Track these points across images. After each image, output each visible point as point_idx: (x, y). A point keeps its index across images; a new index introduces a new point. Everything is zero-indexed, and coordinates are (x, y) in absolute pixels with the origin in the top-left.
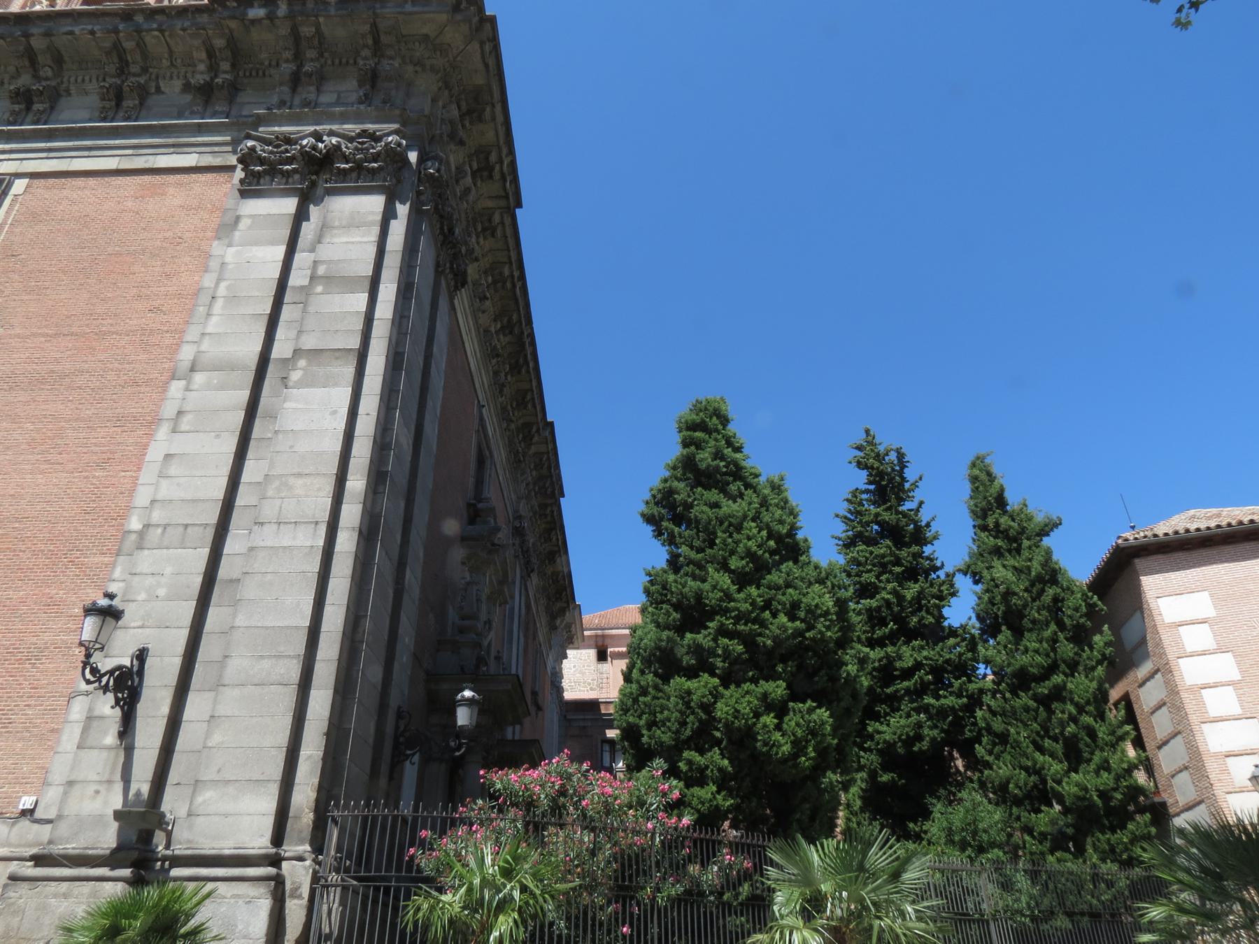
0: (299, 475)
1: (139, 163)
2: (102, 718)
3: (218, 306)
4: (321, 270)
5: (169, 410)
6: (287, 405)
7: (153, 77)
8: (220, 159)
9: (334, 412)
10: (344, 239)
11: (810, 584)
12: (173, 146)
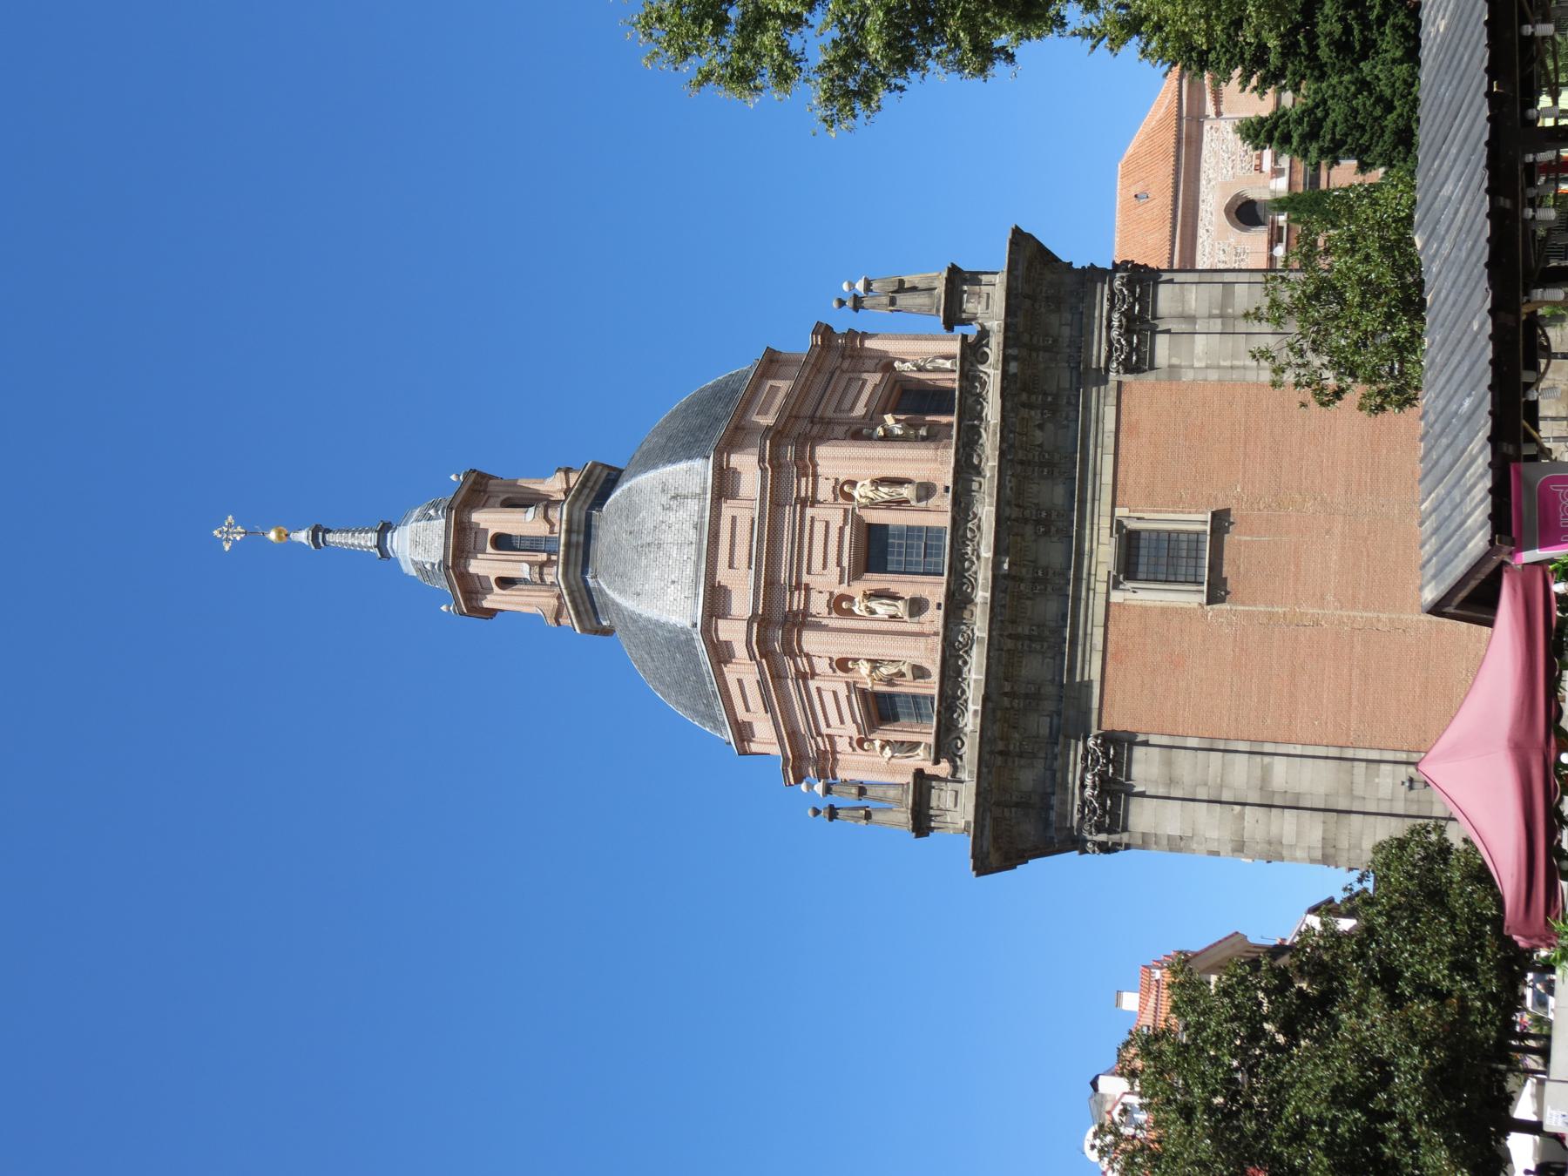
1: (1109, 441)
3: (1236, 363)
4: (1216, 312)
10: (1193, 303)
11: (1393, 75)
12: (1097, 423)
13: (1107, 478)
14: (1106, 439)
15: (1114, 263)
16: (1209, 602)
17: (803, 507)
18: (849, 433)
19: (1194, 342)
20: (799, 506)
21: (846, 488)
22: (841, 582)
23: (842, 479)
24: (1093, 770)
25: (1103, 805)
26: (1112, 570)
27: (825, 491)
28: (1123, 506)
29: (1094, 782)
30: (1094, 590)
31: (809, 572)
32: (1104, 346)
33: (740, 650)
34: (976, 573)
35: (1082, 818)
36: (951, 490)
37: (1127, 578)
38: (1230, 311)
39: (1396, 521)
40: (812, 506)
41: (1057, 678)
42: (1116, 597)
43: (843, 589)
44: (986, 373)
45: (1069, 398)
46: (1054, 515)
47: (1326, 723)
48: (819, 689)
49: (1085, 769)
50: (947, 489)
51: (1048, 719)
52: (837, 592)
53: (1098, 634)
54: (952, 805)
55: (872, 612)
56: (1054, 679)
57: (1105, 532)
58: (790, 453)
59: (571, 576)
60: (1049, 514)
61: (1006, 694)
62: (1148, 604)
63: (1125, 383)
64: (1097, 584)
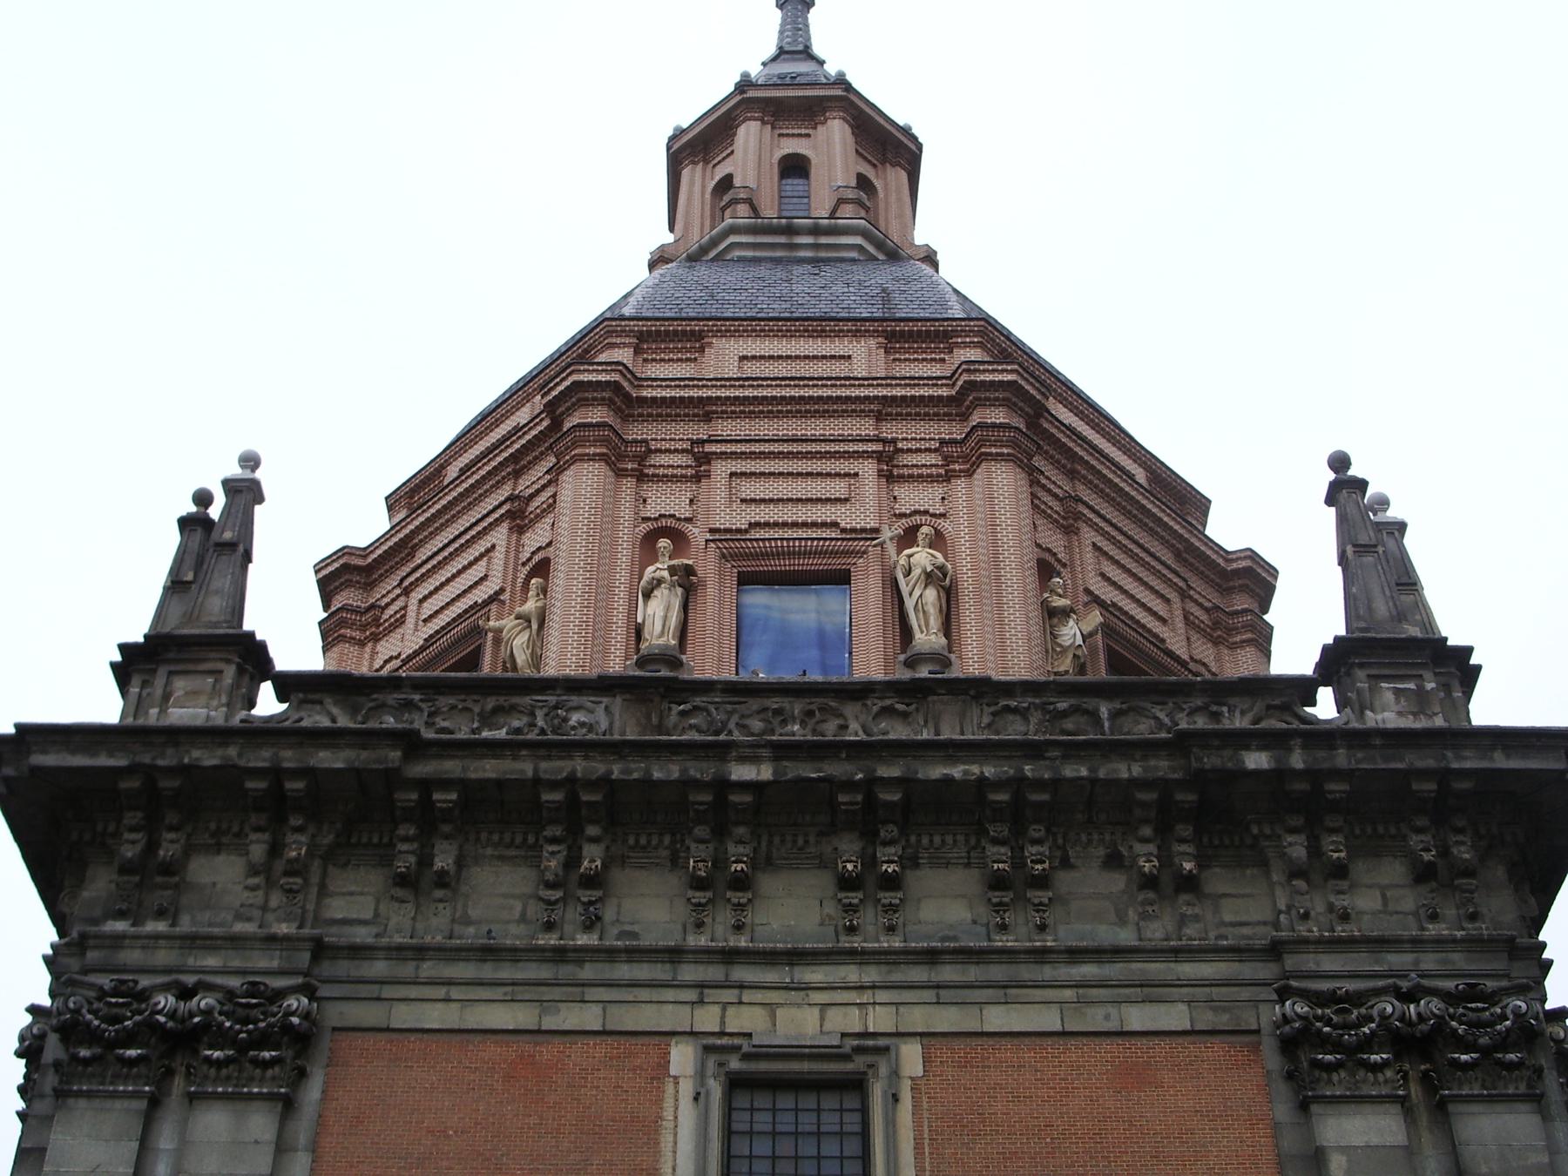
1: (1096, 1019)
7: (1060, 841)
8: (1225, 1017)
13: (998, 1018)
17: (879, 457)
18: (1047, 556)
21: (925, 529)
22: (712, 531)
23: (944, 525)
26: (756, 1041)
29: (192, 1015)
30: (701, 1002)
31: (732, 474)
35: (102, 994)
37: (736, 1084)
40: (880, 473)
42: (682, 1058)
43: (697, 534)
48: (493, 546)
51: (368, 915)
52: (690, 529)
53: (589, 1018)
55: (647, 595)
57: (851, 1021)
58: (998, 416)
59: (733, 239)
62: (666, 1140)
63: (1256, 1048)
64: (716, 1009)
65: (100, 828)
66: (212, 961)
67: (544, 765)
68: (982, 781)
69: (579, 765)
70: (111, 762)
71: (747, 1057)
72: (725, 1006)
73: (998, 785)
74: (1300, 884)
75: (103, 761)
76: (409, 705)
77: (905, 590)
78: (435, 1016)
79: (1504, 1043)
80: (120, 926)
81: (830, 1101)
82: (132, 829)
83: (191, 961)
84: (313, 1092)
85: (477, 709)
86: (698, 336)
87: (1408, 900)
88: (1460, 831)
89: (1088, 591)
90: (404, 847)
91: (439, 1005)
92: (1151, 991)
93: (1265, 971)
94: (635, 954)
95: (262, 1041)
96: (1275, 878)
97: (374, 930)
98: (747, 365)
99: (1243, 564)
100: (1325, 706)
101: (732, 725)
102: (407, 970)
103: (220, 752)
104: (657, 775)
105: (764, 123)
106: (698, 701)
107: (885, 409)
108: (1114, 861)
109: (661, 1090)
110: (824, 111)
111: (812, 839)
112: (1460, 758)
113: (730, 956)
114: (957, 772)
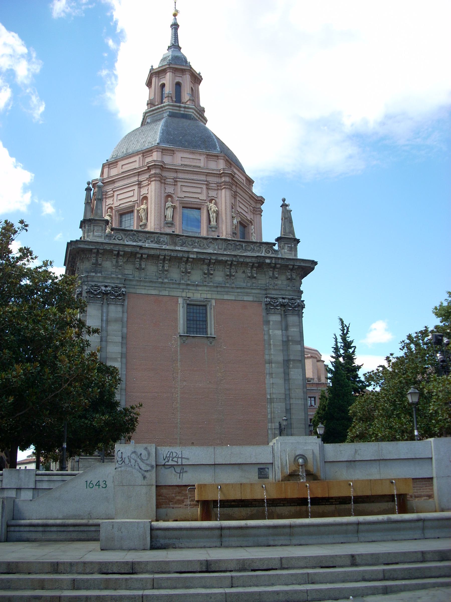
0: (297, 389)
1: (239, 298)
2: (276, 434)
3: (272, 346)
4: (290, 338)
5: (267, 371)
6: (291, 373)
9: (300, 375)
13: (226, 297)
14: (240, 297)
15: (304, 301)
16: (180, 336)
17: (206, 185)
19: (278, 330)
20: (206, 183)
21: (214, 201)
24: (112, 290)
25: (98, 294)
27: (212, 194)
28: (216, 303)
30: (183, 292)
32: (276, 296)
33: (148, 160)
34: (187, 247)
35: (92, 286)
36: (218, 237)
37: (188, 305)
38: (291, 343)
39: (216, 409)
41: (148, 277)
42: (180, 301)
44: (262, 252)
45: (255, 283)
46: (211, 276)
47: (135, 383)
48: (134, 190)
49: (113, 288)
50: (218, 236)
51: (131, 273)
53: (166, 293)
54: (95, 235)
55: (167, 209)
56: (147, 276)
57: (204, 296)
58: (227, 179)
60: (212, 274)
61: (142, 256)
63: (261, 304)
65: (87, 256)
66: (109, 281)
67: (161, 252)
68: (227, 260)
69: (166, 252)
70: (92, 247)
71: (190, 301)
72: (186, 292)
73: (229, 261)
74: (270, 279)
75: (91, 247)
76: (134, 234)
77: (210, 213)
78: (143, 292)
79: (295, 307)
80: (94, 274)
81: (201, 308)
82: (94, 257)
83: (105, 281)
84: (126, 303)
85: (145, 236)
86: (173, 151)
87: (285, 283)
88: (294, 273)
89: (237, 211)
90: (137, 263)
91: (144, 290)
92: (248, 294)
93: (264, 292)
94: (173, 284)
95: (119, 295)
96: (267, 277)
97: (133, 276)
98: (183, 159)
99: (260, 199)
100: (276, 247)
101: (186, 243)
102: (138, 284)
103: (110, 247)
104: (178, 255)
105: (173, 72)
106: (181, 237)
107: (207, 174)
108: (244, 272)
109: (177, 305)
110: (185, 72)
111: (200, 265)
112: (296, 263)
113: (188, 285)
114: (224, 258)
